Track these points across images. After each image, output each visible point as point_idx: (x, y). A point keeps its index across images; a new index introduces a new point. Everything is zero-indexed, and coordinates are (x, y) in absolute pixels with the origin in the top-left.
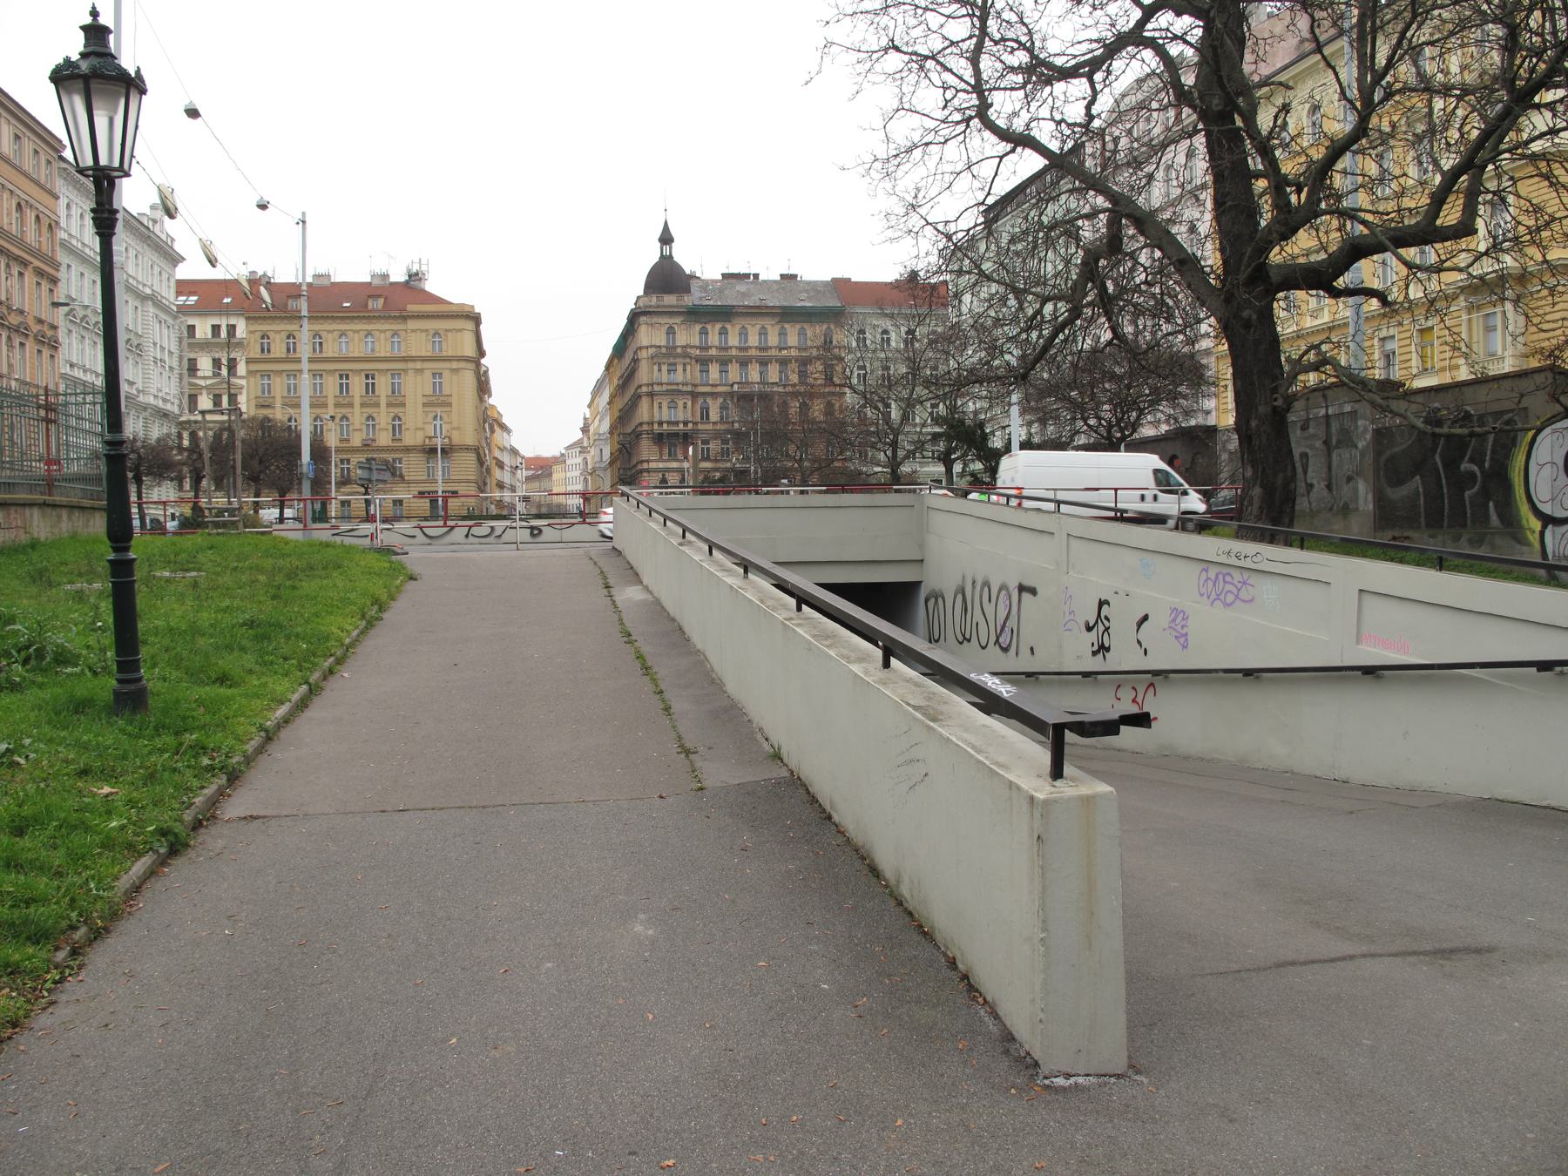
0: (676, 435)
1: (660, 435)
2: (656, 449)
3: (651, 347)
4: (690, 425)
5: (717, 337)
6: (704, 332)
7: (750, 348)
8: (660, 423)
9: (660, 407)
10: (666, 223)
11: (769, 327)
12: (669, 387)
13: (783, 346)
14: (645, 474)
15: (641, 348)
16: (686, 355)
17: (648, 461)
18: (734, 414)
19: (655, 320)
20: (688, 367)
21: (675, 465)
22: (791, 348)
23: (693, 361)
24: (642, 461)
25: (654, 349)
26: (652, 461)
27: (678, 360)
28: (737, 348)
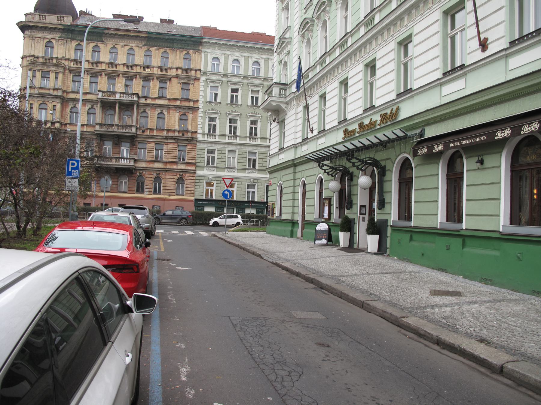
3: (30, 56)
5: (90, 54)
6: (79, 48)
7: (119, 64)
11: (136, 49)
12: (42, 91)
13: (148, 64)
16: (59, 65)
18: (98, 118)
19: (36, 34)
20: (60, 76)
22: (154, 67)
23: (67, 71)
27: (52, 69)
28: (106, 63)
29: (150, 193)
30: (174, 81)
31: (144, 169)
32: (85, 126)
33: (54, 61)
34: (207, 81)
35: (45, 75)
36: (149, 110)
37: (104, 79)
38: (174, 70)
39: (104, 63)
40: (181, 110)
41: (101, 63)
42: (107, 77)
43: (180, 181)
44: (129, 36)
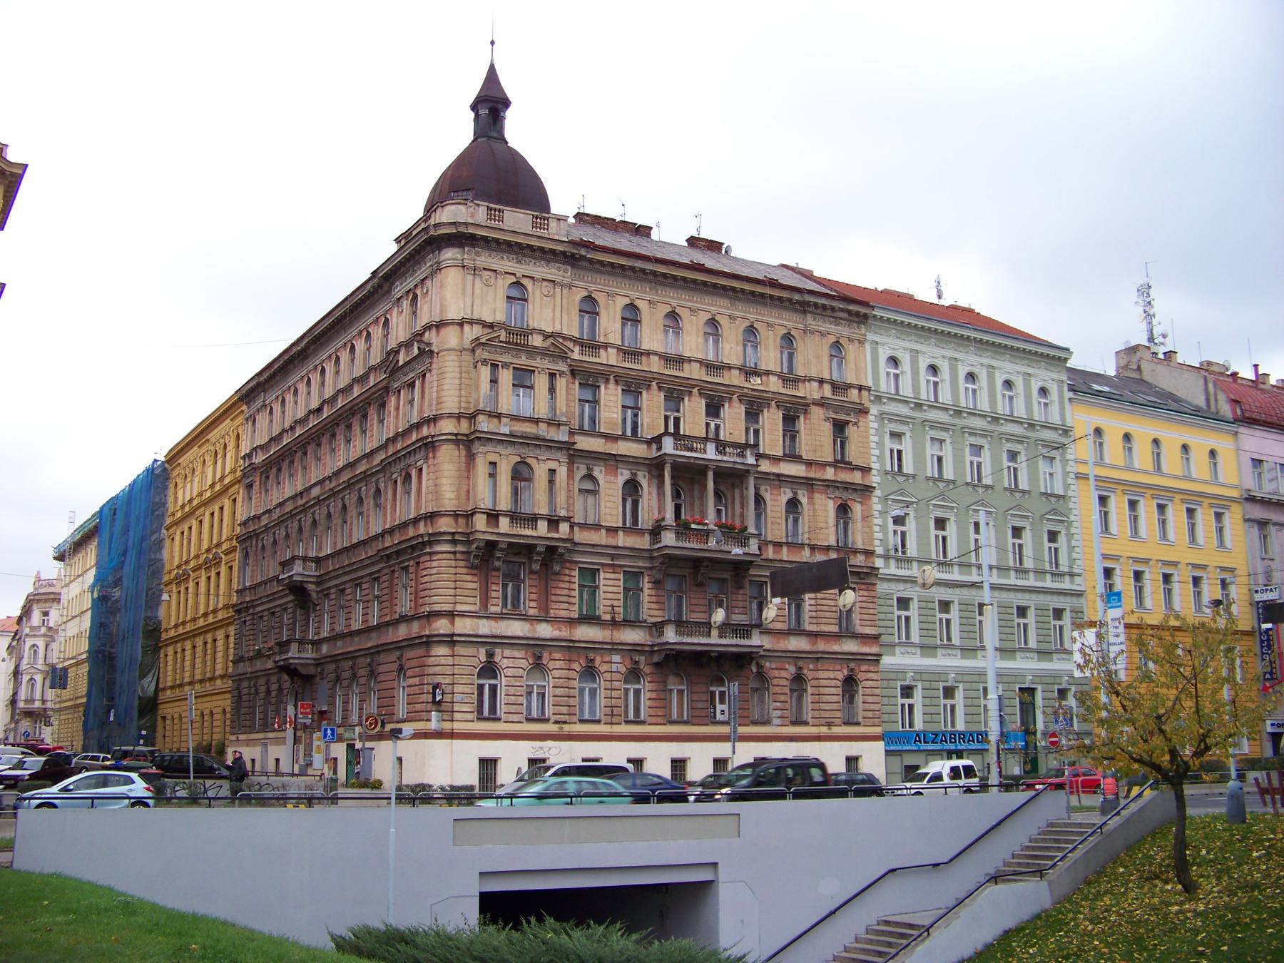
0: (525, 550)
1: (491, 545)
2: (471, 584)
3: (472, 322)
4: (564, 528)
6: (590, 307)
8: (493, 516)
9: (492, 475)
10: (492, 70)
14: (442, 650)
15: (439, 325)
17: (451, 615)
19: (485, 259)
20: (561, 383)
21: (516, 628)
22: (768, 373)
24: (439, 614)
25: (477, 331)
26: (463, 615)
29: (515, 718)
30: (817, 412)
31: (771, 654)
32: (620, 533)
33: (536, 341)
34: (881, 416)
35: (523, 379)
36: (766, 490)
37: (656, 398)
38: (815, 384)
39: (655, 353)
40: (838, 494)
42: (662, 395)
43: (850, 683)
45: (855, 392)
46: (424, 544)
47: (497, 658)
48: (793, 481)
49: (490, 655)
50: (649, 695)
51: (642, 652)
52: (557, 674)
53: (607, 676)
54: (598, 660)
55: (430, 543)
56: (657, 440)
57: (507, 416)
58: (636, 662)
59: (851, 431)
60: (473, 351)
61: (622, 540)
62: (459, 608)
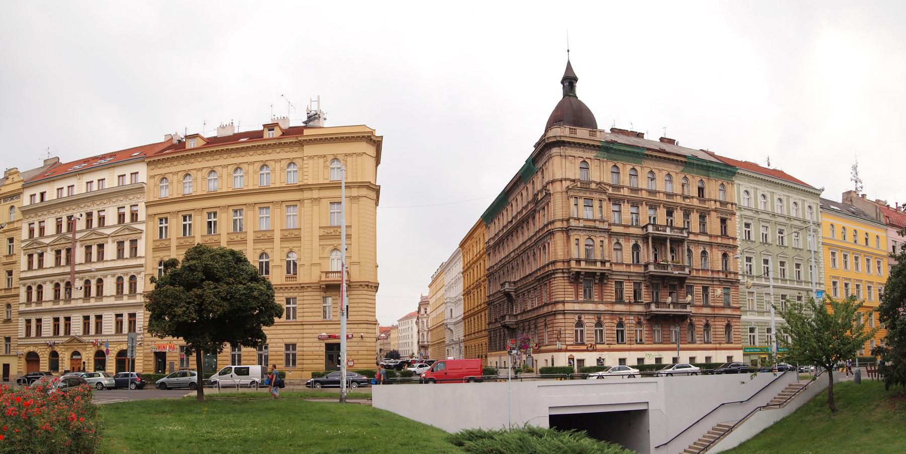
2: (571, 289)
3: (566, 179)
4: (608, 265)
5: (628, 178)
6: (616, 172)
8: (578, 261)
14: (560, 317)
15: (553, 182)
17: (563, 302)
19: (570, 151)
20: (604, 204)
22: (693, 197)
26: (568, 302)
30: (713, 214)
31: (695, 315)
32: (632, 266)
33: (593, 186)
36: (693, 247)
37: (645, 209)
39: (644, 190)
40: (722, 249)
41: (641, 190)
42: (648, 207)
43: (728, 327)
44: (669, 159)
45: (730, 206)
46: (552, 274)
47: (583, 319)
48: (704, 243)
49: (580, 318)
50: (645, 332)
51: (642, 315)
52: (607, 324)
53: (628, 325)
54: (624, 318)
55: (554, 274)
56: (646, 227)
57: (582, 219)
58: (640, 319)
59: (728, 222)
60: (567, 192)
61: (632, 269)
62: (566, 299)
